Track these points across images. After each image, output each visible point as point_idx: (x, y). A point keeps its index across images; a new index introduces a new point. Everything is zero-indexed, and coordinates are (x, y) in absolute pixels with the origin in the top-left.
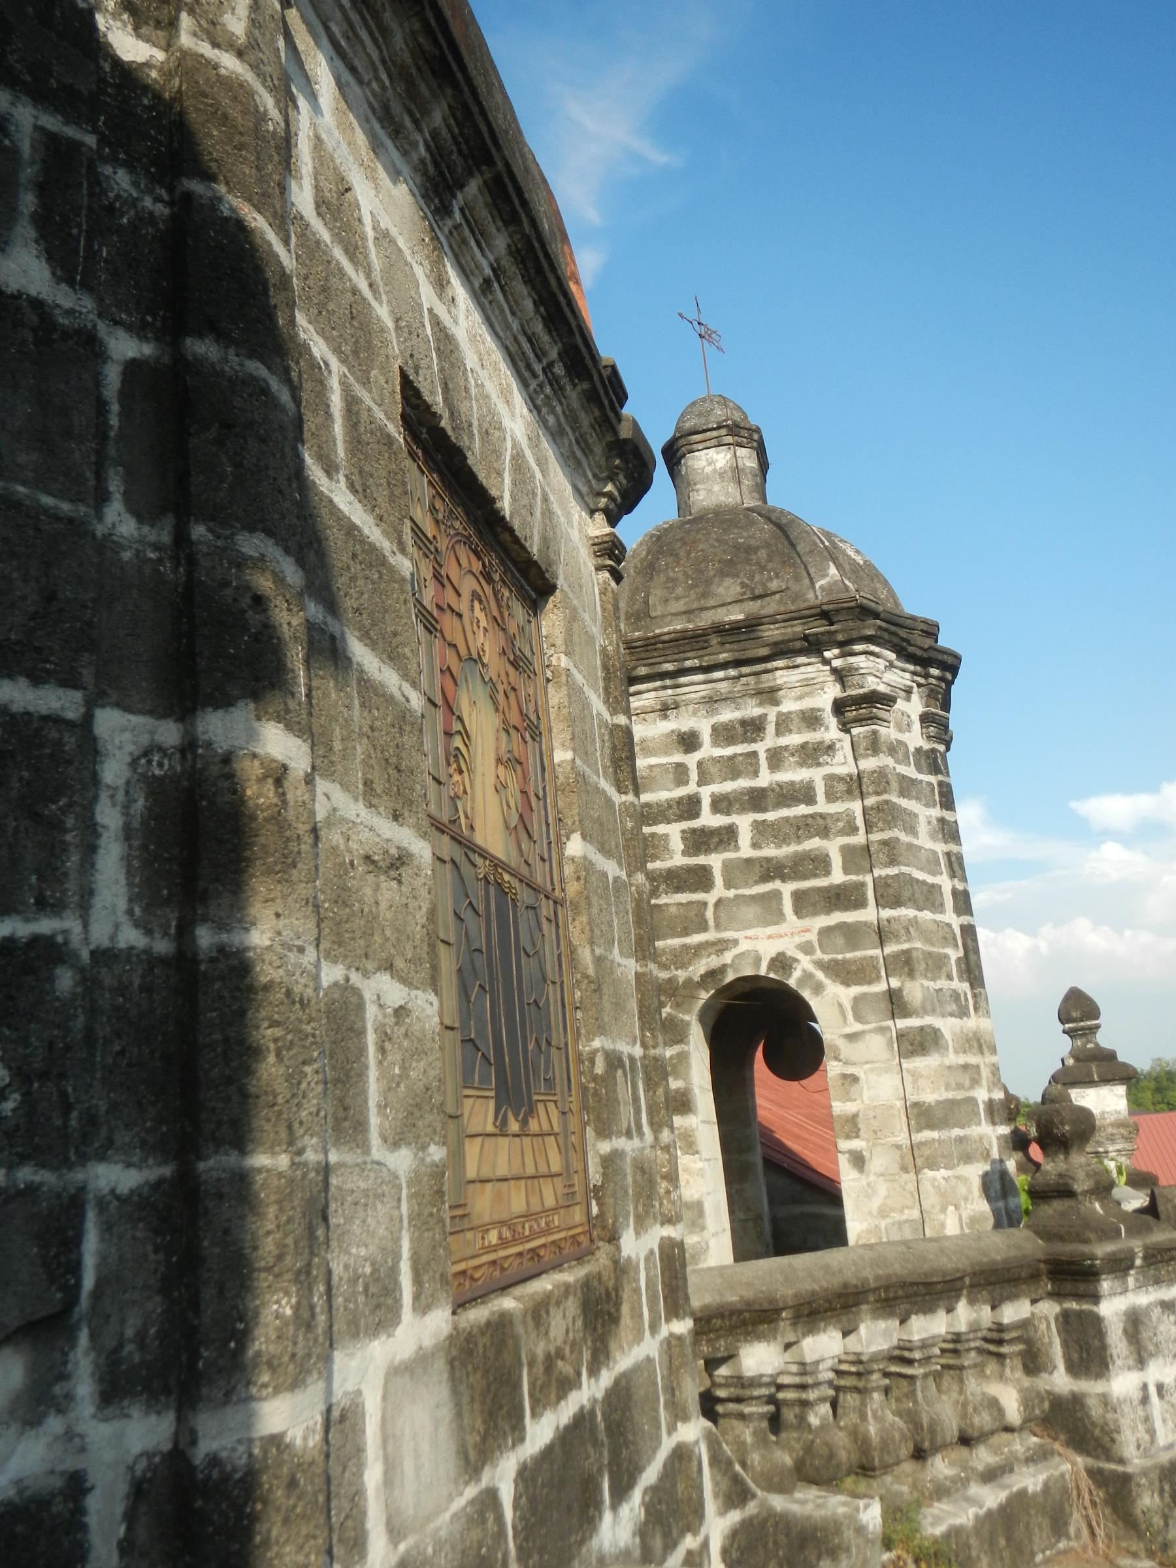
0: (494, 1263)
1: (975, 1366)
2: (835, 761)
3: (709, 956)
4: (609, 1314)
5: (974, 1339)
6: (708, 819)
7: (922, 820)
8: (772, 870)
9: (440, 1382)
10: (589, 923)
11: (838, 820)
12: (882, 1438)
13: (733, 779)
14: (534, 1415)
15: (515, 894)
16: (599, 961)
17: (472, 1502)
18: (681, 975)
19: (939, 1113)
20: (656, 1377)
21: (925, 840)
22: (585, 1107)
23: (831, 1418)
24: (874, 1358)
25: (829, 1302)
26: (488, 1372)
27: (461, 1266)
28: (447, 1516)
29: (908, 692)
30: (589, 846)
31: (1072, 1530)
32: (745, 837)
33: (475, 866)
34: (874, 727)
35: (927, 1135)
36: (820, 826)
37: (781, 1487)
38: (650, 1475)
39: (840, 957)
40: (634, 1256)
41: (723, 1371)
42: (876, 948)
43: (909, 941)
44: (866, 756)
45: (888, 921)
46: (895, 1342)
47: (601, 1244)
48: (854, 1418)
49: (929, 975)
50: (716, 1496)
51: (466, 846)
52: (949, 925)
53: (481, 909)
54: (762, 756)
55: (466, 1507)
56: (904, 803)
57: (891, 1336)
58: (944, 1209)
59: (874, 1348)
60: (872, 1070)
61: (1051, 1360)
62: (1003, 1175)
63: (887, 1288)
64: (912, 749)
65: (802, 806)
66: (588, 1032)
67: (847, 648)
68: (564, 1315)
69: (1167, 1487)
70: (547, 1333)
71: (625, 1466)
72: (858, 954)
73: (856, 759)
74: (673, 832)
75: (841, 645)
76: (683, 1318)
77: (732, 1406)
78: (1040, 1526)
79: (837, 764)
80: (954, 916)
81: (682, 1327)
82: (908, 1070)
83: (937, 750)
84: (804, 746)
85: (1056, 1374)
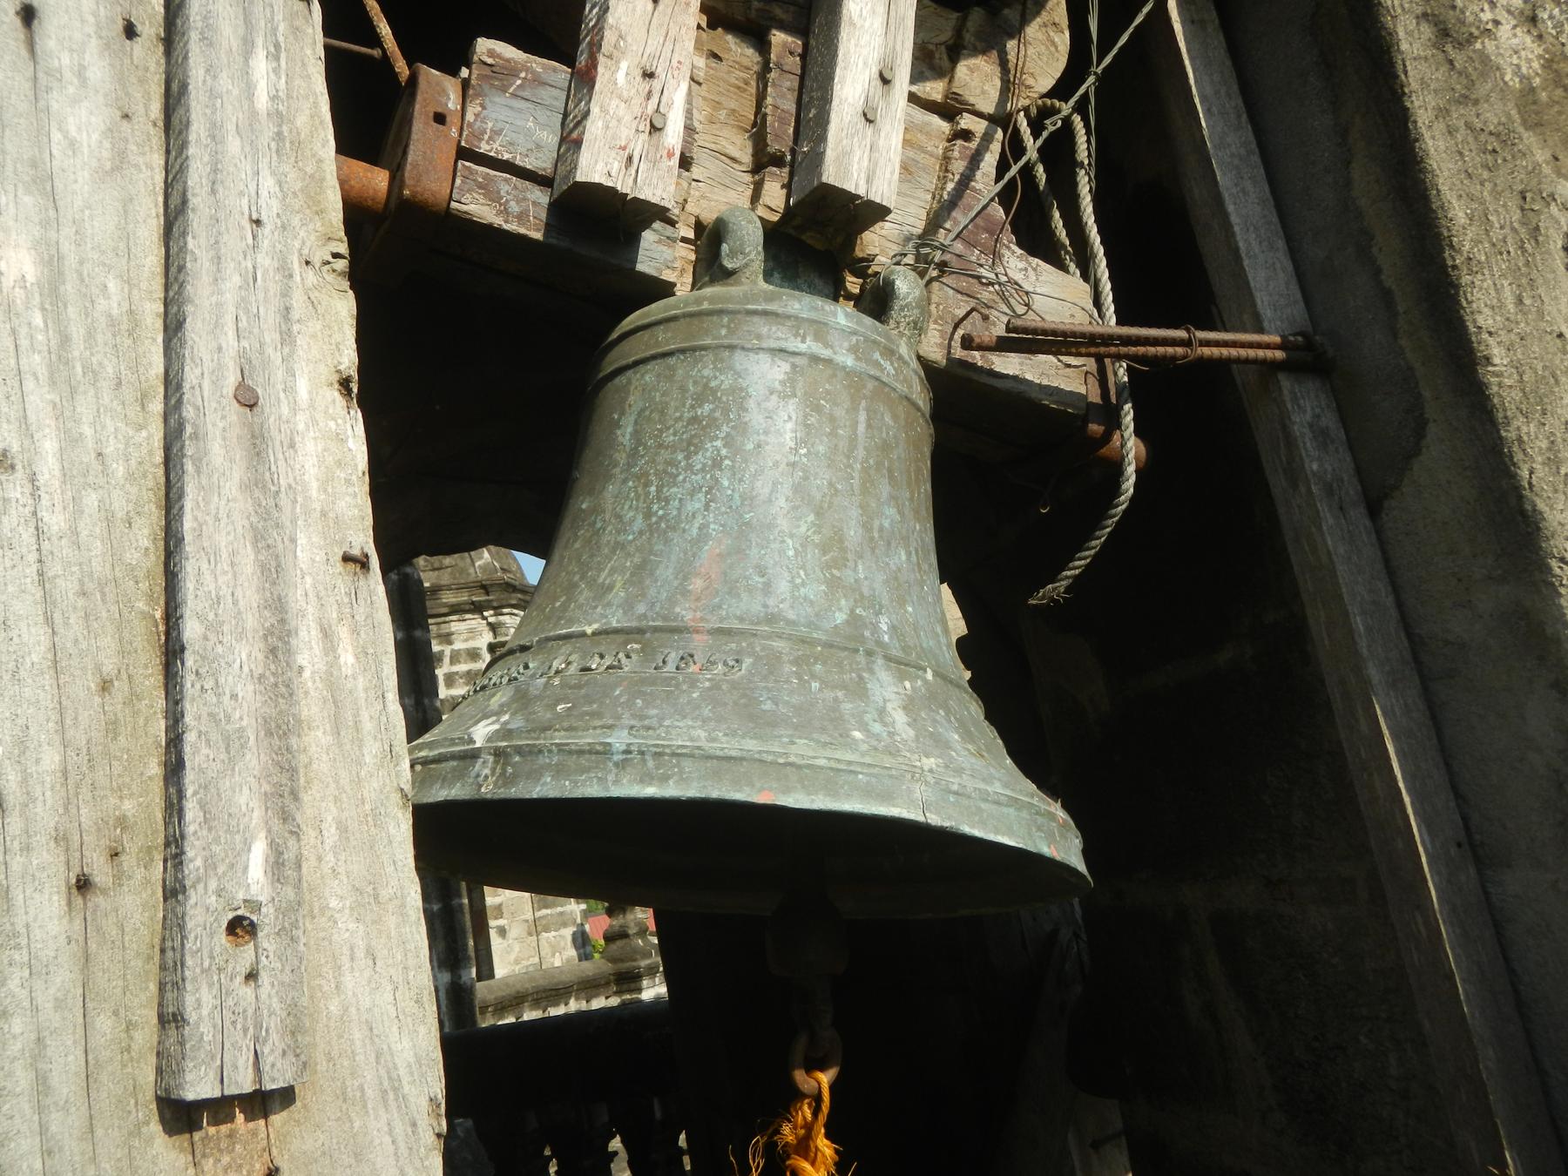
25: (510, 1001)
58: (553, 955)
63: (537, 993)
67: (499, 611)
75: (494, 608)
84: (469, 672)
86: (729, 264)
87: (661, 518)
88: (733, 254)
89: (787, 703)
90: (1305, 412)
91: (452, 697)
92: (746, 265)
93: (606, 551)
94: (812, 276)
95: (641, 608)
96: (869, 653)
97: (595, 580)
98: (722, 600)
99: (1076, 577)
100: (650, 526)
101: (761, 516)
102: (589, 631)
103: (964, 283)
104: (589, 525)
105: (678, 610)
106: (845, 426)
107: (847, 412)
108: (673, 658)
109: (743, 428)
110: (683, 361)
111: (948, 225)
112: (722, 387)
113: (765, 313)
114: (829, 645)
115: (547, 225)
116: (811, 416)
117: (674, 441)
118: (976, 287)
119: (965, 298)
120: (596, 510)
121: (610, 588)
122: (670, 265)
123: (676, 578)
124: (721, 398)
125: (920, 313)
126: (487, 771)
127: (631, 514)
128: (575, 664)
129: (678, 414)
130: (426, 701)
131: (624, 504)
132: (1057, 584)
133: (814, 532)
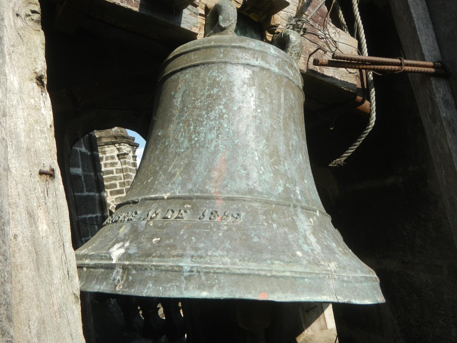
29: (130, 151)
36: (115, 178)
73: (121, 165)
75: (119, 143)
84: (111, 163)
86: (223, 25)
87: (196, 141)
88: (224, 20)
89: (264, 237)
90: (440, 93)
91: (107, 171)
92: (230, 26)
93: (171, 156)
94: (252, 32)
95: (190, 186)
96: (295, 206)
97: (167, 171)
98: (227, 182)
99: (348, 156)
100: (191, 145)
101: (243, 141)
102: (166, 197)
103: (313, 38)
104: (162, 143)
105: (207, 187)
106: (276, 99)
107: (276, 93)
108: (207, 213)
109: (232, 100)
110: (203, 69)
111: (306, 13)
112: (222, 81)
113: (240, 47)
114: (278, 204)
115: (141, 4)
116: (262, 94)
117: (201, 105)
118: (317, 40)
119: (313, 44)
120: (165, 136)
121: (174, 175)
122: (195, 25)
123: (205, 171)
124: (221, 86)
125: (300, 50)
126: (119, 277)
127: (182, 139)
128: (160, 214)
129: (202, 93)
130: (98, 174)
131: (178, 134)
132: (341, 159)
133: (266, 149)
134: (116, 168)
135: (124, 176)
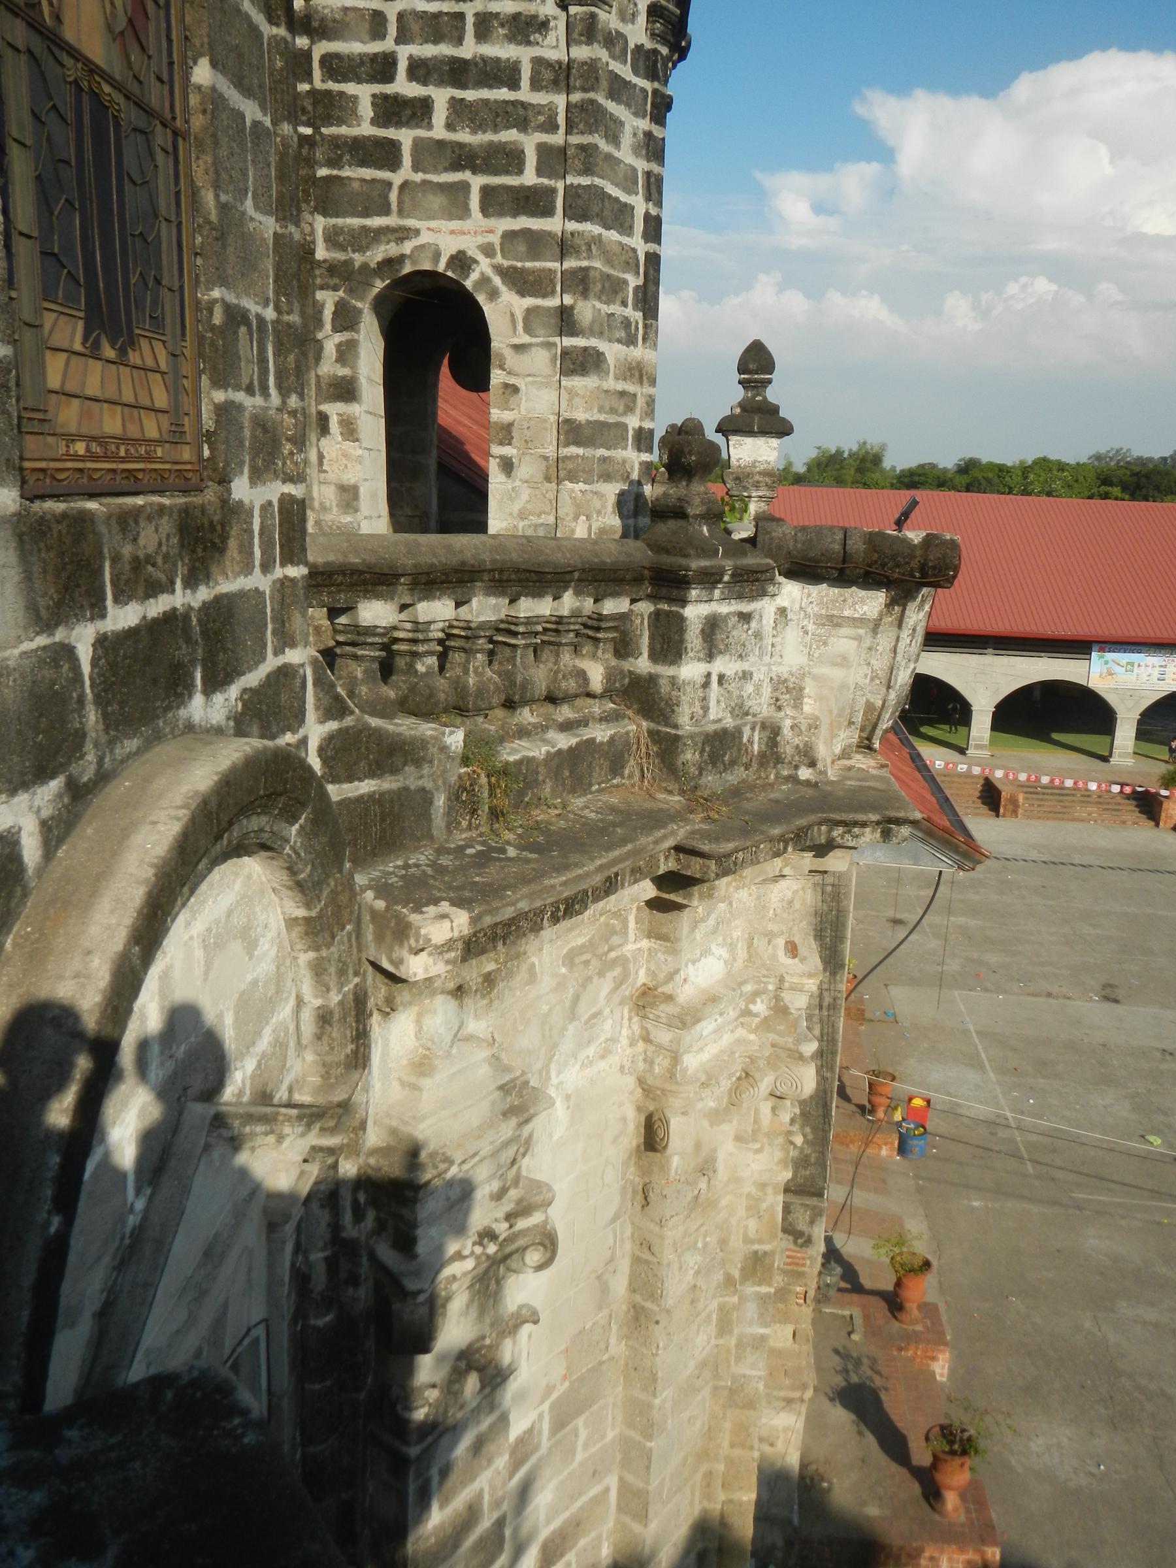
0: (81, 470)
1: (571, 644)
2: (546, 42)
3: (388, 243)
4: (213, 544)
5: (574, 624)
6: (403, 86)
7: (628, 130)
8: (463, 158)
9: (7, 549)
10: (214, 164)
11: (539, 113)
12: (478, 687)
13: (436, 42)
14: (116, 600)
15: (118, 111)
16: (223, 208)
17: (44, 648)
18: (358, 259)
19: (587, 432)
20: (266, 607)
21: (627, 154)
22: (201, 355)
23: (436, 669)
24: (482, 626)
25: (445, 574)
26: (63, 553)
27: (43, 465)
28: (16, 652)
30: (220, 76)
31: (627, 772)
32: (440, 115)
33: (62, 66)
34: (593, 9)
35: (574, 450)
37: (382, 715)
38: (253, 679)
39: (519, 265)
40: (246, 501)
41: (343, 620)
42: (556, 261)
43: (589, 258)
44: (579, 43)
45: (572, 234)
46: (503, 616)
47: (210, 483)
48: (459, 671)
49: (604, 298)
50: (317, 708)
51: (48, 38)
52: (634, 251)
53: (70, 116)
54: (470, 21)
55: (36, 650)
56: (611, 106)
57: (499, 611)
58: (576, 518)
59: (482, 619)
60: (532, 383)
61: (639, 648)
62: (639, 496)
63: (501, 571)
64: (631, 45)
65: (505, 90)
66: (207, 280)
68: (157, 530)
69: (707, 749)
70: (135, 540)
71: (222, 666)
72: (537, 264)
73: (568, 46)
74: (363, 93)
76: (298, 565)
77: (348, 648)
78: (601, 769)
79: (548, 46)
80: (641, 242)
81: (296, 572)
82: (565, 388)
83: (659, 52)
84: (516, 16)
85: (640, 659)
91: (484, 59)
134: (536, 52)
135: (569, 106)
